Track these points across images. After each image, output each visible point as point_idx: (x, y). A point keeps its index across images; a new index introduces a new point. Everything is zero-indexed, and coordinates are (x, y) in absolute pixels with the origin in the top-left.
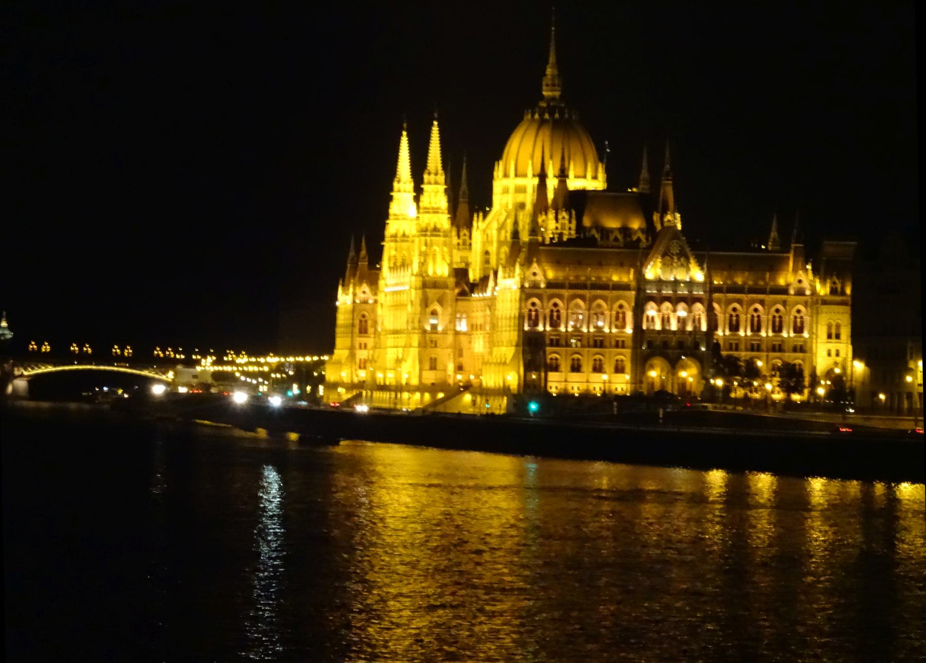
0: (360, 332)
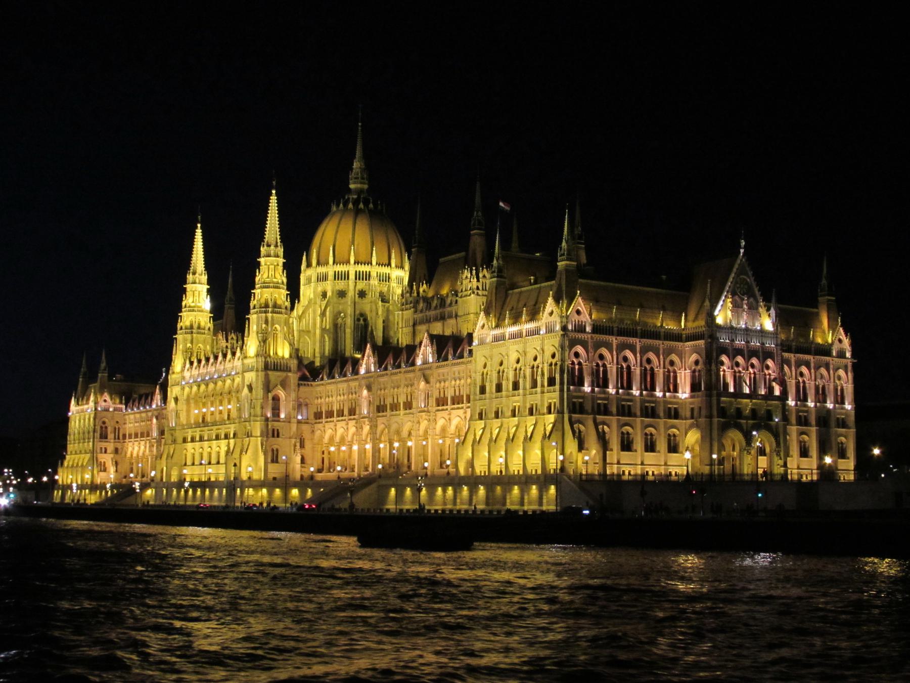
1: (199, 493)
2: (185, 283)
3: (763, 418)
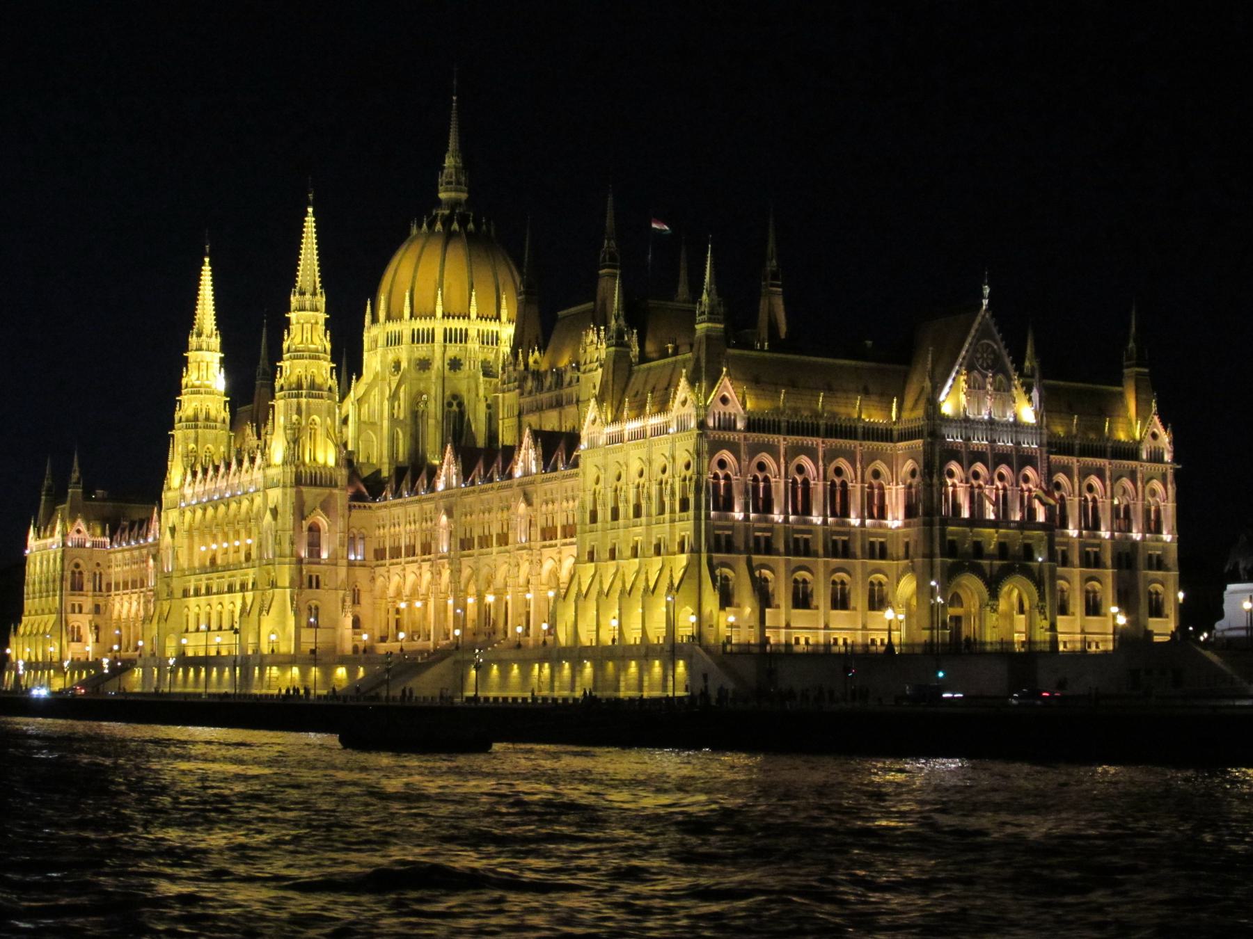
0: (73, 589)
1: (203, 674)
2: (187, 350)
3: (1010, 560)
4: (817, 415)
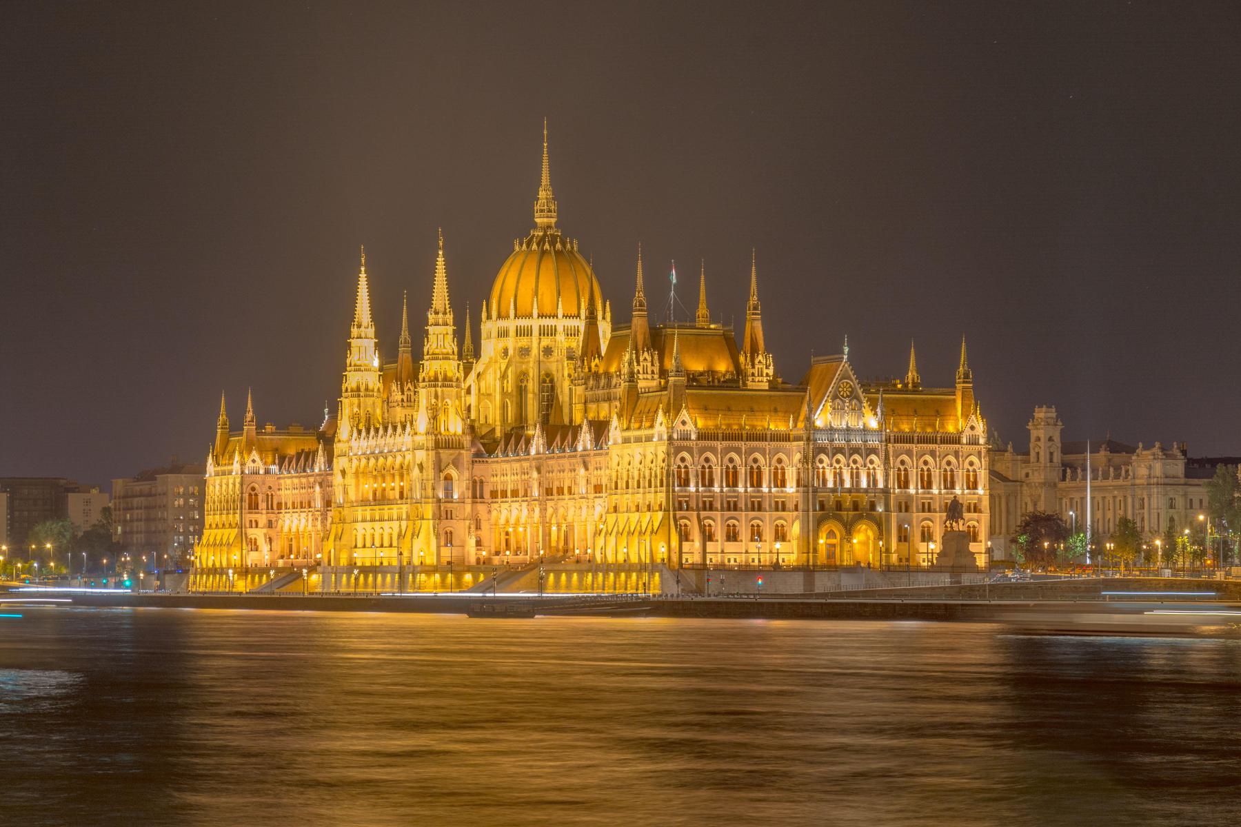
0: (250, 508)
4: (742, 428)
